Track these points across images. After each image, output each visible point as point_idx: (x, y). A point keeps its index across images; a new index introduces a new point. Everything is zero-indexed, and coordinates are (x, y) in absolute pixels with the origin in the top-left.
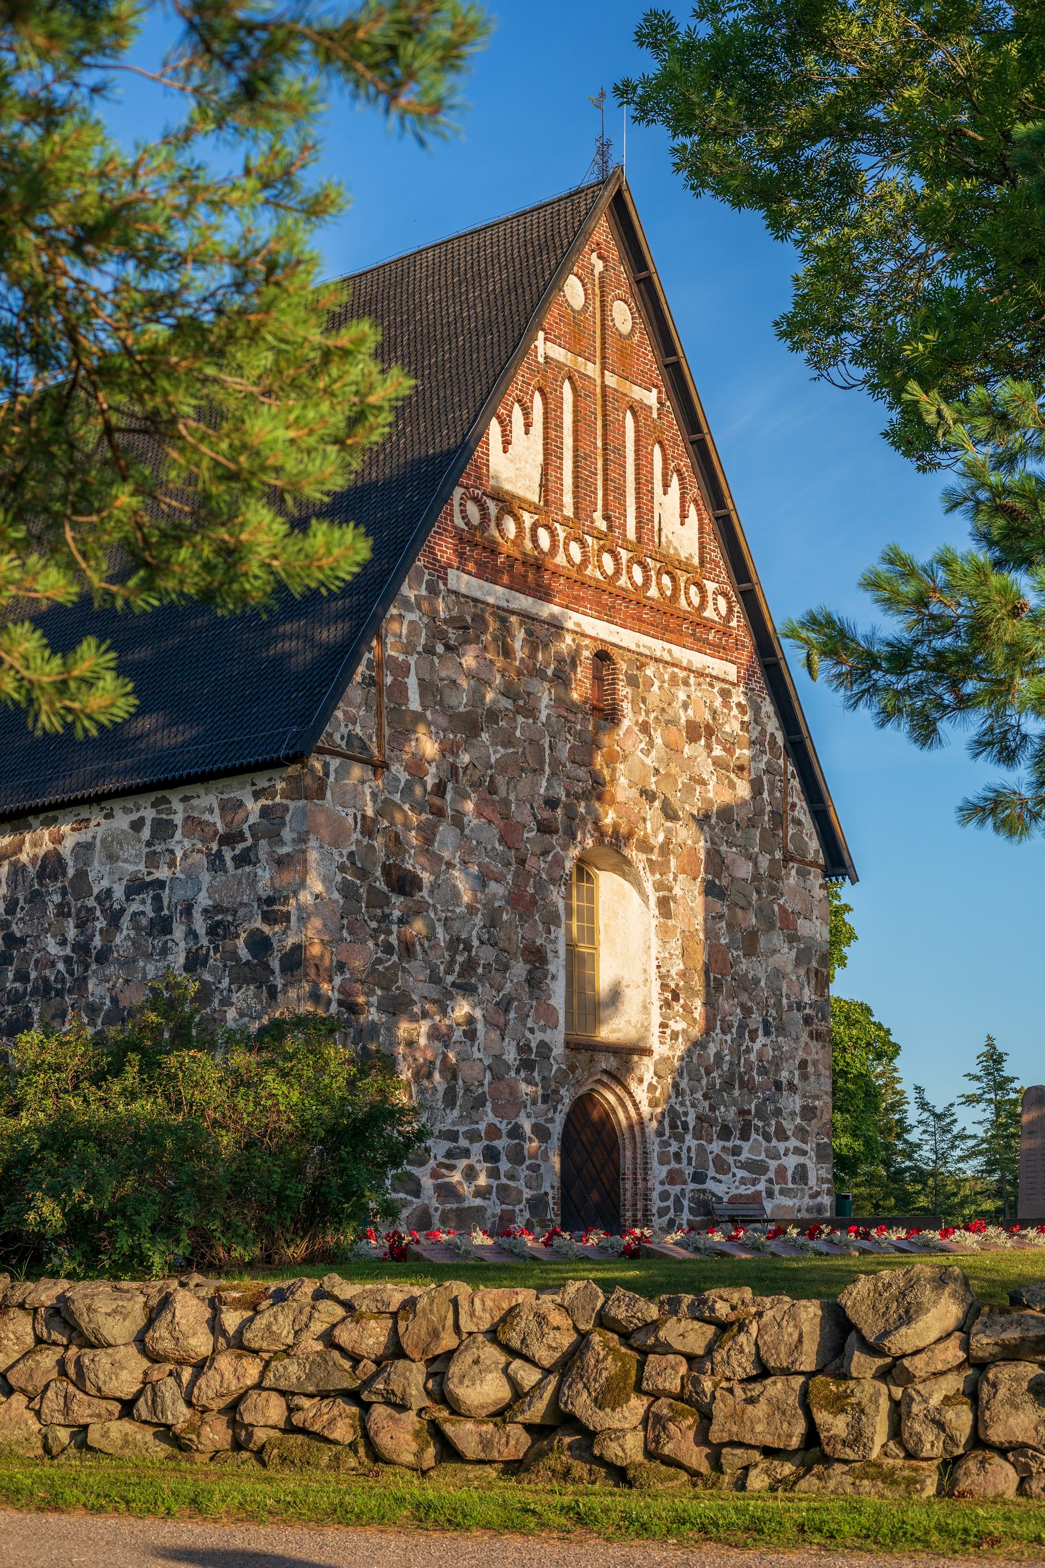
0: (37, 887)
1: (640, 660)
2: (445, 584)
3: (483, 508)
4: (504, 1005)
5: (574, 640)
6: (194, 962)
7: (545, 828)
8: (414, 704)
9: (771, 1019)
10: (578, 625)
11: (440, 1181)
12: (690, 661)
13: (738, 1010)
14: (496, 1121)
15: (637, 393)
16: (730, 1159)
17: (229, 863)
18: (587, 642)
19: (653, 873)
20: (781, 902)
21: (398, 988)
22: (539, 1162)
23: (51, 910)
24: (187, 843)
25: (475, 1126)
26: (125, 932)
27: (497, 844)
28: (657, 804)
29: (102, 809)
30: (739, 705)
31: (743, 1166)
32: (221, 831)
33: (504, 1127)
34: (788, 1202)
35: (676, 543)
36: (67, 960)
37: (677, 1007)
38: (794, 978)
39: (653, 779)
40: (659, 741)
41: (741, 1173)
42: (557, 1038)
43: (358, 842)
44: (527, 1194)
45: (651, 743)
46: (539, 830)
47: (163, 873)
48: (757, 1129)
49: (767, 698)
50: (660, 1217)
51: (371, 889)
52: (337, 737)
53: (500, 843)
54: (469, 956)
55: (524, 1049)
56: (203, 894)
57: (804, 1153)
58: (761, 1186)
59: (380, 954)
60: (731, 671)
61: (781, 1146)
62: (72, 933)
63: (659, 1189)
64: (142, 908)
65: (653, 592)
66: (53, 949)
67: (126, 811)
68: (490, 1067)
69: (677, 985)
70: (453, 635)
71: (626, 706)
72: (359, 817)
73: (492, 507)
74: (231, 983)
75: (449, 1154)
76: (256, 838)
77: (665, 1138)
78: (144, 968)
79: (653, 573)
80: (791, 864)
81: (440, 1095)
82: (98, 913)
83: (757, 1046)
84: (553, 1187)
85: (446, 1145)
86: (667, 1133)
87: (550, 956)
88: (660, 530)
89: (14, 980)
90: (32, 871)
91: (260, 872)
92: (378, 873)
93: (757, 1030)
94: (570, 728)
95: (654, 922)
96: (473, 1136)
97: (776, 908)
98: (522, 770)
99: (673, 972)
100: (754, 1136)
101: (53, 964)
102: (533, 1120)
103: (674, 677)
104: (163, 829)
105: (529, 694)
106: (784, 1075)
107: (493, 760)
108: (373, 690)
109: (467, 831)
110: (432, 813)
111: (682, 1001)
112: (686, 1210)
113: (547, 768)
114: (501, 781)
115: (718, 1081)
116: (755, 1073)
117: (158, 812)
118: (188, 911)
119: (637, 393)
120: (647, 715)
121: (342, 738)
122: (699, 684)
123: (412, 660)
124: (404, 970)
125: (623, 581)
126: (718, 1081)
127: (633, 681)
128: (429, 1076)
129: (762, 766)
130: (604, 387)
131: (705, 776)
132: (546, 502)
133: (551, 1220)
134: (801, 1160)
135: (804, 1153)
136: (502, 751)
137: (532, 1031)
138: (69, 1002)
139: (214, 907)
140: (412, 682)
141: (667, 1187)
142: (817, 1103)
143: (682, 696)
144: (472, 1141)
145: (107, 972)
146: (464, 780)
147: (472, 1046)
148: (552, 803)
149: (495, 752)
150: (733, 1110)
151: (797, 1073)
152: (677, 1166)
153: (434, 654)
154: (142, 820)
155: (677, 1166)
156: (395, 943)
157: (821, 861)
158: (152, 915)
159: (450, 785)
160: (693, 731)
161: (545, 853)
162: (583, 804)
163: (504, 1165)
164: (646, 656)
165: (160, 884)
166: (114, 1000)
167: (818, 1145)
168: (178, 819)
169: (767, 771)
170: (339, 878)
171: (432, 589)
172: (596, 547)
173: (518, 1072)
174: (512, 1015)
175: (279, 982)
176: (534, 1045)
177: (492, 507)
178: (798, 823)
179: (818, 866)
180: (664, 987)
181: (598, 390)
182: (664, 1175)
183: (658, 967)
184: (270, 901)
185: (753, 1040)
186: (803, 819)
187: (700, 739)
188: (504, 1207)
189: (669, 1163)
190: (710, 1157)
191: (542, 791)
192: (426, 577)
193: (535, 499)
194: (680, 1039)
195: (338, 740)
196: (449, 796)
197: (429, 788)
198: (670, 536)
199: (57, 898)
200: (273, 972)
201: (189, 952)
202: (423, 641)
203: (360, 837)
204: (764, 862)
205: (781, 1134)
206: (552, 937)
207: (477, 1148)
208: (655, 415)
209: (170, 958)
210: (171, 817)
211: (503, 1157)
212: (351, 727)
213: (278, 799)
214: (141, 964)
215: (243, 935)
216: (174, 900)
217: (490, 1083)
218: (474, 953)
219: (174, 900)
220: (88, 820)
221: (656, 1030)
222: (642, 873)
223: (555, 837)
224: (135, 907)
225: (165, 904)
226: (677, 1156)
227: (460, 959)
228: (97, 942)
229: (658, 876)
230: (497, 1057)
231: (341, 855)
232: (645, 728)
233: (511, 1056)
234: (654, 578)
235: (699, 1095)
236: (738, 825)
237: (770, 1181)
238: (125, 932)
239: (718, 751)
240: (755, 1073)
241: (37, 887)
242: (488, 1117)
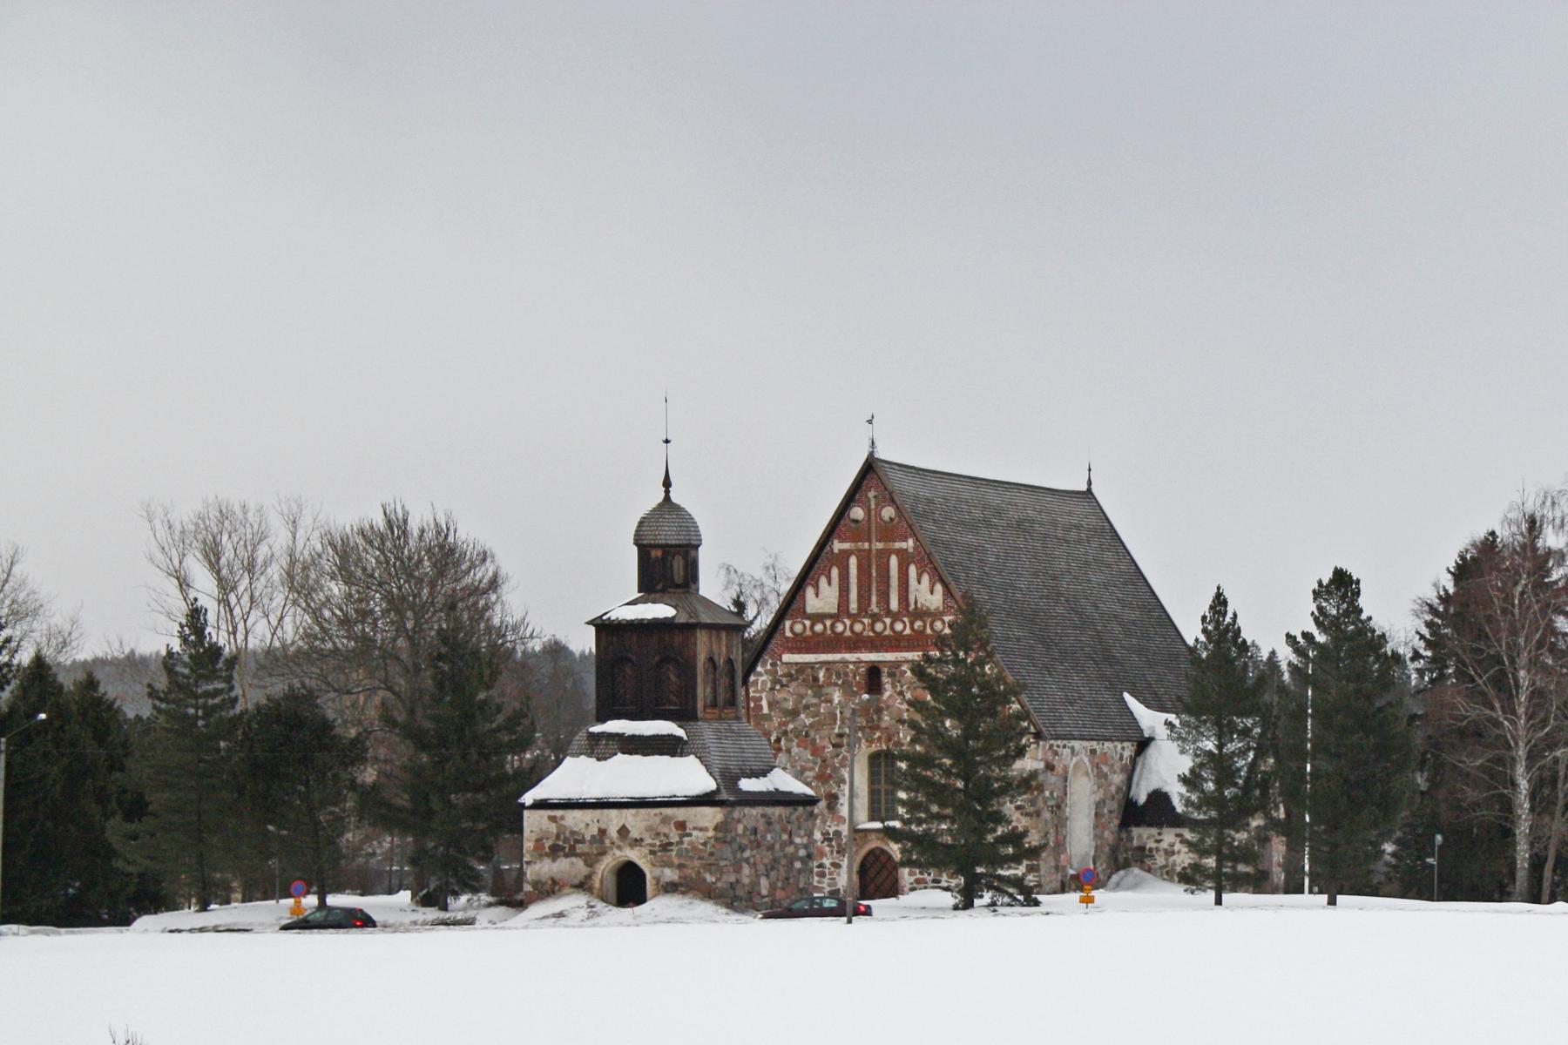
8: (766, 710)
10: (858, 658)
22: (828, 876)
35: (928, 604)
55: (825, 834)
70: (784, 680)
71: (888, 687)
87: (840, 796)
102: (831, 861)
107: (808, 724)
109: (793, 754)
114: (812, 733)
120: (902, 686)
127: (891, 675)
137: (830, 826)
140: (764, 703)
146: (791, 735)
152: (921, 877)
161: (837, 756)
171: (774, 665)
173: (823, 842)
176: (831, 832)
198: (923, 602)
206: (842, 788)
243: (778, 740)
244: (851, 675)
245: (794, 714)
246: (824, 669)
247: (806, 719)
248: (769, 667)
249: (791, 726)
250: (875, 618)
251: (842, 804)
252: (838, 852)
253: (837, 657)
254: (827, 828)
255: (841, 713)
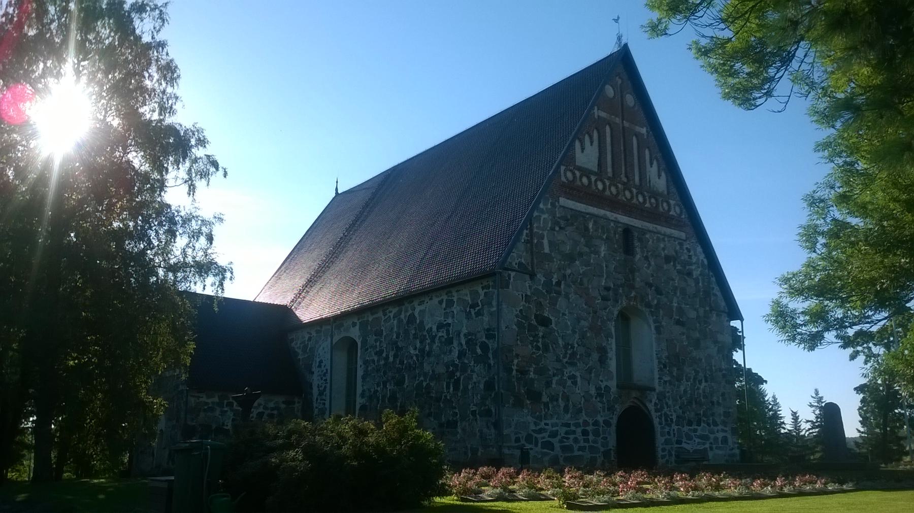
0: (406, 328)
1: (643, 232)
2: (559, 203)
3: (574, 174)
4: (589, 371)
5: (614, 224)
6: (461, 354)
7: (605, 299)
8: (547, 250)
9: (708, 376)
11: (563, 444)
12: (665, 232)
13: (693, 372)
14: (587, 419)
15: (638, 129)
16: (693, 434)
17: (473, 315)
18: (620, 225)
19: (653, 316)
20: (710, 327)
21: (542, 364)
23: (411, 337)
24: (458, 308)
25: (577, 421)
26: (437, 344)
27: (584, 305)
28: (653, 288)
29: (429, 296)
30: (687, 248)
31: (699, 437)
32: (470, 303)
33: (591, 422)
34: (720, 452)
36: (417, 355)
37: (666, 371)
38: (717, 358)
39: (651, 279)
40: (653, 263)
41: (697, 440)
42: (613, 384)
43: (524, 306)
44: (602, 449)
45: (649, 265)
46: (602, 300)
47: (450, 321)
48: (704, 421)
49: (699, 245)
50: (662, 459)
51: (530, 325)
52: (514, 264)
53: (586, 305)
54: (573, 351)
55: (598, 389)
56: (465, 328)
57: (726, 431)
58: (707, 446)
59: (534, 351)
60: (683, 235)
61: (716, 428)
62: (418, 345)
63: (661, 447)
64: (442, 335)
65: (647, 205)
66: (412, 352)
67: (437, 296)
68: (583, 396)
69: (665, 362)
70: (562, 223)
71: (638, 250)
72: (524, 296)
73: (578, 173)
74: (474, 364)
75: (567, 433)
76: (483, 306)
77: (663, 426)
78: (443, 358)
79: (647, 197)
80: (713, 312)
81: (562, 408)
82: (427, 337)
83: (702, 387)
84: (613, 446)
85: (565, 429)
86: (664, 424)
87: (609, 350)
88: (650, 181)
89: (399, 364)
90: (405, 321)
91: (484, 318)
92: (533, 318)
93: (702, 380)
94: (614, 259)
95: (654, 336)
96: (577, 425)
97: (707, 329)
98: (594, 276)
99: (663, 357)
100: (702, 424)
101: (412, 358)
102: (603, 418)
103: (658, 239)
104: (450, 303)
105: (596, 246)
106: (715, 399)
107: (581, 272)
108: (528, 245)
109: (571, 300)
110: (555, 293)
111: (668, 368)
112: (674, 456)
113: (605, 274)
114: (585, 280)
115: (685, 401)
116: (702, 398)
117: (448, 296)
118: (459, 335)
119: (638, 129)
121: (516, 264)
122: (669, 241)
123: (545, 233)
124: (545, 356)
125: (634, 201)
126: (685, 401)
127: (640, 240)
128: (557, 400)
129: (699, 272)
130: (623, 127)
131: (674, 277)
132: (601, 172)
133: (613, 461)
134: (724, 434)
135: (726, 431)
136: (585, 268)
138: (417, 372)
139: (468, 333)
140: (545, 242)
141: (664, 446)
142: (730, 410)
143: (662, 245)
144: (577, 427)
145: (430, 360)
147: (576, 387)
148: (607, 289)
149: (582, 269)
150: (693, 413)
151: (721, 398)
152: (669, 437)
153: (555, 230)
154: (443, 300)
155: (669, 437)
156: (541, 346)
157: (727, 311)
158: (446, 337)
159: (563, 282)
160: (668, 259)
161: (605, 309)
162: (621, 289)
163: (591, 437)
164: (646, 230)
165: (449, 325)
166: (433, 371)
167: (732, 428)
168: (455, 299)
169: (700, 275)
170: (516, 320)
171: (553, 205)
172: (622, 188)
174: (593, 375)
175: (492, 362)
176: (603, 387)
177: (578, 173)
178: (715, 295)
179: (725, 313)
180: (660, 362)
181: (621, 128)
182: (663, 441)
183: (656, 354)
184: (488, 330)
185: (700, 384)
186: (717, 293)
187: (671, 262)
188: (592, 455)
189: (665, 436)
190: (684, 433)
191: (603, 284)
192: (550, 201)
193: (596, 170)
194: (668, 384)
195: (515, 266)
196: (562, 286)
197: (554, 283)
199: (413, 332)
200: (490, 358)
201: (459, 351)
202: (550, 225)
203: (524, 303)
204: (701, 311)
205: (715, 424)
206: (609, 343)
207: (579, 430)
208: (646, 137)
209: (452, 354)
210: (453, 298)
211: (591, 434)
212: (519, 260)
213: (491, 289)
214: (442, 356)
215: (479, 344)
216: (454, 331)
217: (584, 403)
218: (575, 349)
219: (454, 331)
220: (424, 301)
221: (657, 381)
222: (648, 316)
223: (609, 302)
224: (440, 334)
225: (451, 333)
226: (669, 433)
227: (569, 352)
228: (427, 348)
229: (655, 317)
230: (587, 392)
231: (517, 311)
232: (646, 258)
233: (593, 391)
234: (648, 200)
235: (677, 407)
236: (689, 297)
237: (711, 443)
238: (437, 344)
239: (679, 267)
240: (702, 398)
241: (406, 328)
242: (583, 417)
243: (559, 284)
244: (612, 232)
245: (571, 258)
246: (592, 221)
247: (579, 267)
248: (549, 206)
249: (569, 271)
250: (627, 186)
251: (611, 359)
252: (609, 409)
253: (602, 212)
254: (600, 383)
255: (606, 266)
